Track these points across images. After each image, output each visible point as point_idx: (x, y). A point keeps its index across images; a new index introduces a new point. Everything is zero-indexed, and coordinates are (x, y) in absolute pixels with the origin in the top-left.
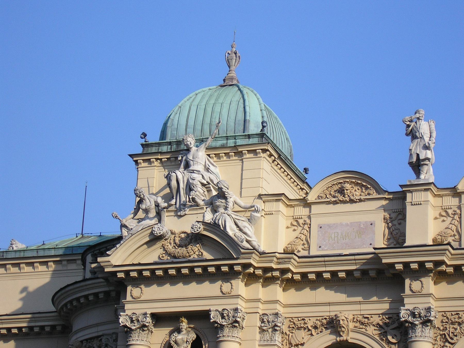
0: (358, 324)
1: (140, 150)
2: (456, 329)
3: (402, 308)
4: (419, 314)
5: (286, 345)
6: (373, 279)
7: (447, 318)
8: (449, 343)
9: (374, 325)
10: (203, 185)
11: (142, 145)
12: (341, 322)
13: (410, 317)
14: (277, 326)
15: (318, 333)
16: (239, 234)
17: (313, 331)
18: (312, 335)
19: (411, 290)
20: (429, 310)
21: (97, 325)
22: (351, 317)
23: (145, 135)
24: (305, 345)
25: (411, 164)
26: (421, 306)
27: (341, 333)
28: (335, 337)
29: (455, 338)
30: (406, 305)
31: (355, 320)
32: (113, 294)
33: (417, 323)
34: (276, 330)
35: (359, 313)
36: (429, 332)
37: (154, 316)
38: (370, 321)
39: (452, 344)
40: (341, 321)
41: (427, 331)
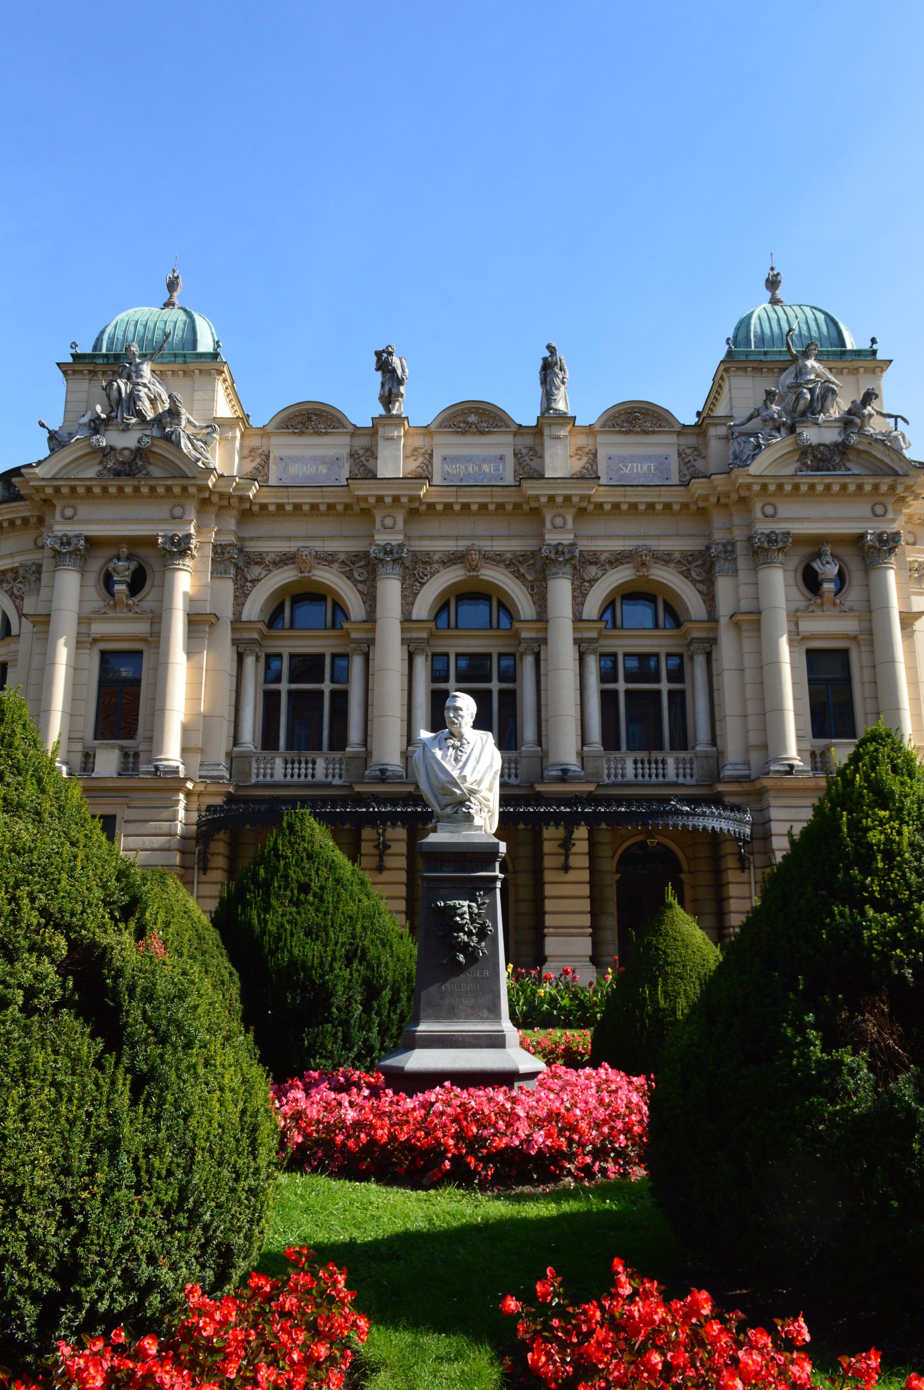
1: (71, 360)
6: (339, 515)
10: (149, 397)
11: (72, 355)
16: (193, 452)
21: (12, 555)
23: (74, 345)
25: (381, 398)
26: (393, 543)
32: (33, 521)
37: (88, 539)
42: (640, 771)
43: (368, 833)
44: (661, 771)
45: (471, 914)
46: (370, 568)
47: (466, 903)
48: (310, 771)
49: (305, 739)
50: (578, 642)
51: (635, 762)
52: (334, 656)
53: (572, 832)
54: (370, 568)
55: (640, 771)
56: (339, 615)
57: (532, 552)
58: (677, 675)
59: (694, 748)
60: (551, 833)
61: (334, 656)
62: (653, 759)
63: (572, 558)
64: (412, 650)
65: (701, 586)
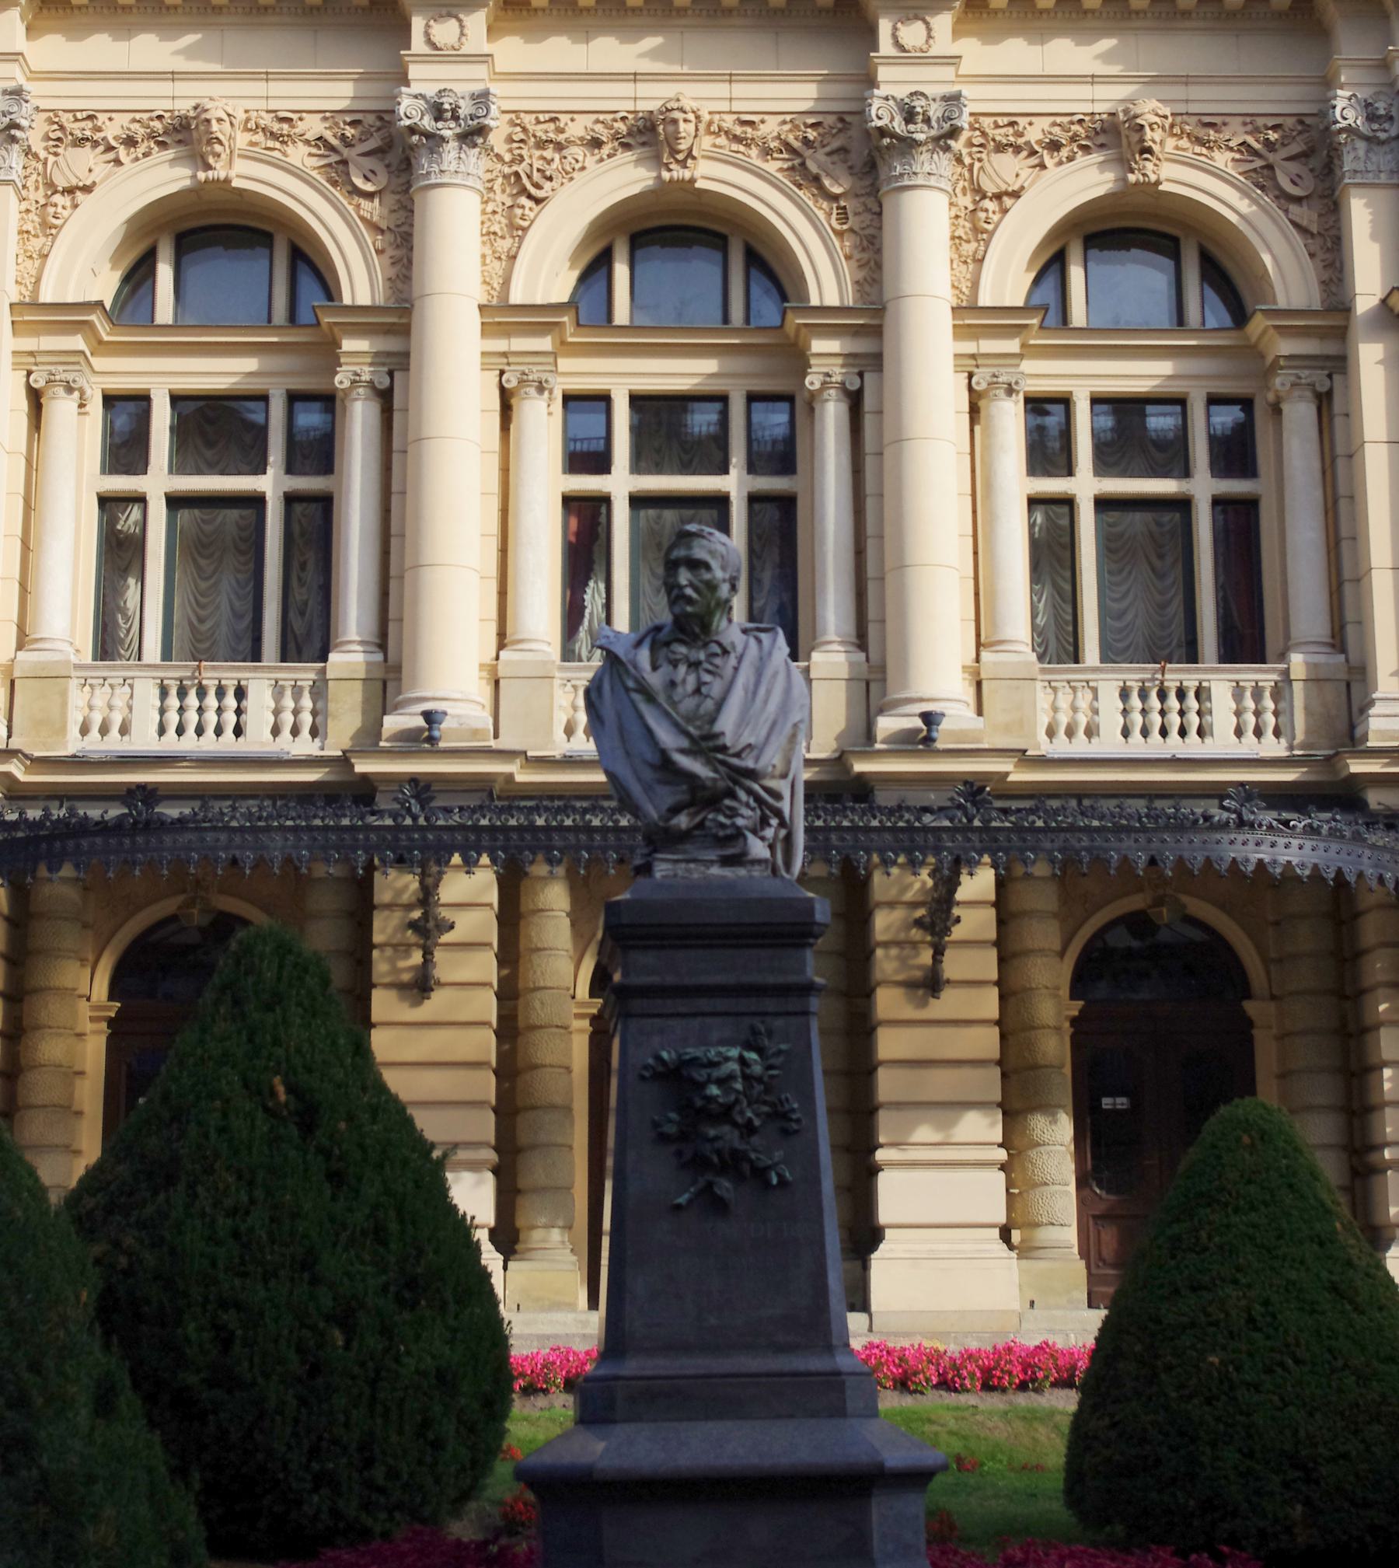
0: (259, 137)
2: (549, 162)
3: (404, 89)
4: (454, 110)
5: (37, 188)
7: (525, 130)
8: (530, 197)
9: (307, 142)
12: (215, 126)
13: (427, 118)
14: (18, 127)
15: (137, 159)
17: (122, 151)
18: (118, 162)
19: (430, 42)
20: (482, 98)
22: (241, 116)
24: (97, 190)
27: (211, 160)
28: (188, 172)
29: (547, 185)
30: (412, 84)
31: (251, 125)
33: (447, 133)
34: (14, 140)
35: (262, 104)
36: (475, 162)
38: (296, 130)
39: (538, 201)
40: (214, 122)
41: (474, 160)
42: (1137, 719)
43: (396, 885)
44: (1194, 720)
45: (746, 1078)
46: (393, 157)
47: (734, 1052)
48: (230, 719)
49: (215, 630)
50: (967, 367)
51: (1125, 694)
52: (294, 398)
53: (953, 883)
54: (393, 157)
55: (1137, 719)
56: (307, 283)
57: (841, 117)
58: (1235, 453)
59: (1282, 657)
60: (898, 889)
61: (294, 398)
62: (1172, 682)
63: (954, 133)
64: (511, 381)
65: (1305, 214)
